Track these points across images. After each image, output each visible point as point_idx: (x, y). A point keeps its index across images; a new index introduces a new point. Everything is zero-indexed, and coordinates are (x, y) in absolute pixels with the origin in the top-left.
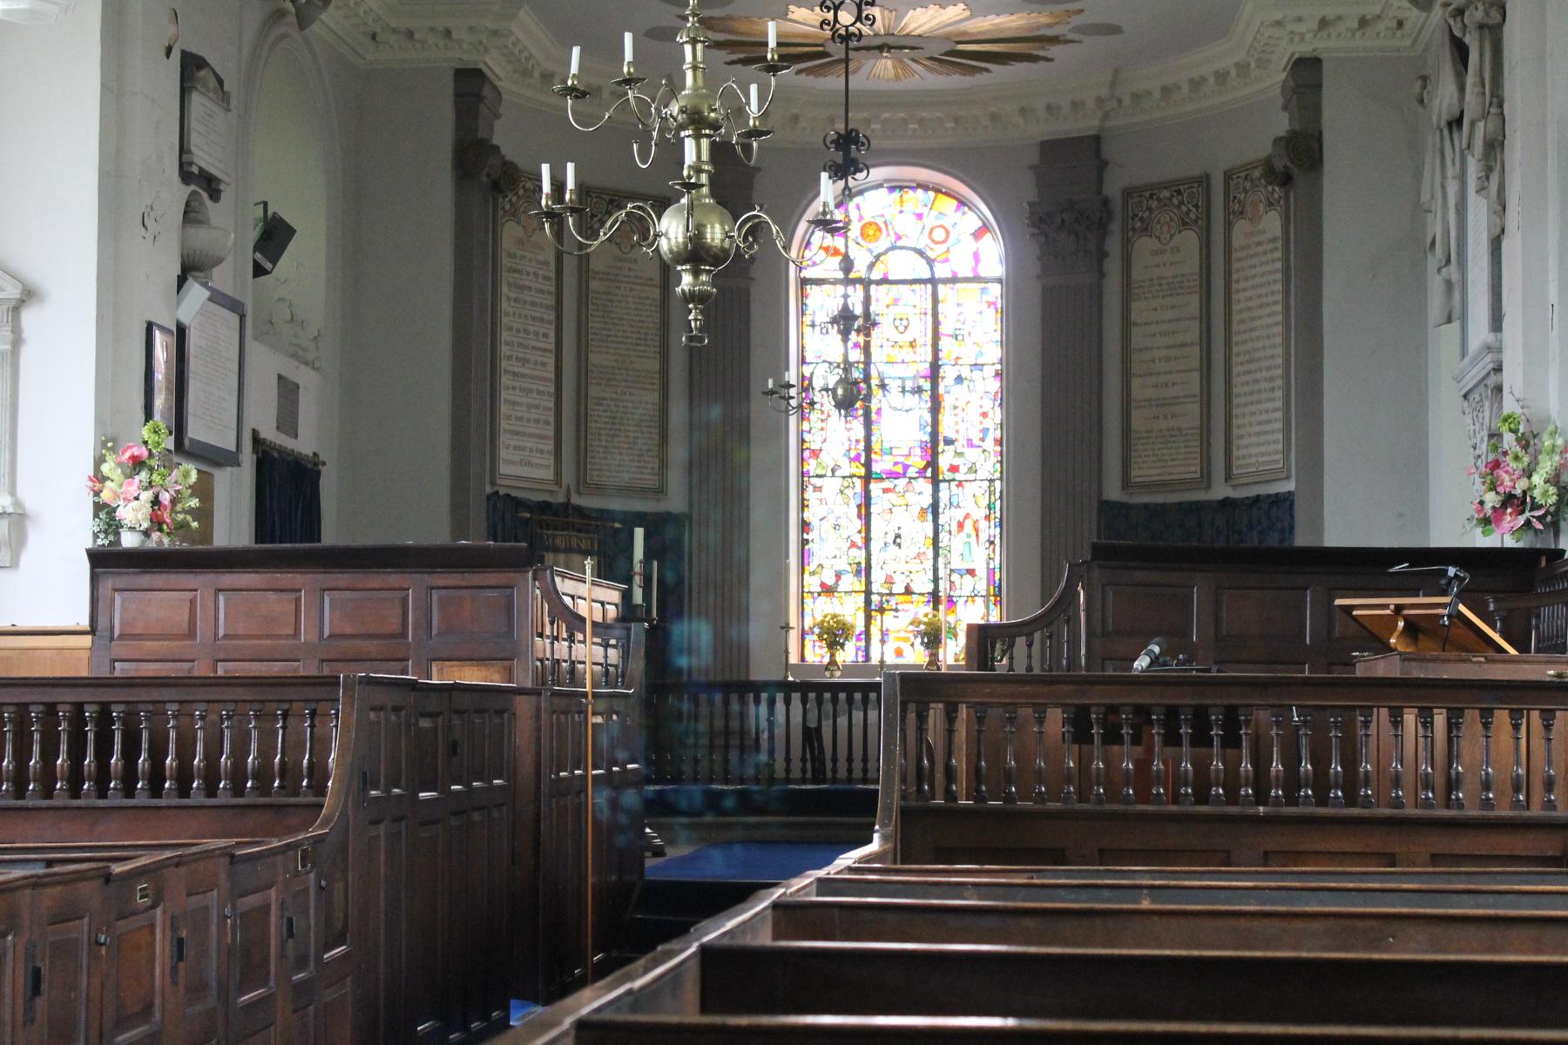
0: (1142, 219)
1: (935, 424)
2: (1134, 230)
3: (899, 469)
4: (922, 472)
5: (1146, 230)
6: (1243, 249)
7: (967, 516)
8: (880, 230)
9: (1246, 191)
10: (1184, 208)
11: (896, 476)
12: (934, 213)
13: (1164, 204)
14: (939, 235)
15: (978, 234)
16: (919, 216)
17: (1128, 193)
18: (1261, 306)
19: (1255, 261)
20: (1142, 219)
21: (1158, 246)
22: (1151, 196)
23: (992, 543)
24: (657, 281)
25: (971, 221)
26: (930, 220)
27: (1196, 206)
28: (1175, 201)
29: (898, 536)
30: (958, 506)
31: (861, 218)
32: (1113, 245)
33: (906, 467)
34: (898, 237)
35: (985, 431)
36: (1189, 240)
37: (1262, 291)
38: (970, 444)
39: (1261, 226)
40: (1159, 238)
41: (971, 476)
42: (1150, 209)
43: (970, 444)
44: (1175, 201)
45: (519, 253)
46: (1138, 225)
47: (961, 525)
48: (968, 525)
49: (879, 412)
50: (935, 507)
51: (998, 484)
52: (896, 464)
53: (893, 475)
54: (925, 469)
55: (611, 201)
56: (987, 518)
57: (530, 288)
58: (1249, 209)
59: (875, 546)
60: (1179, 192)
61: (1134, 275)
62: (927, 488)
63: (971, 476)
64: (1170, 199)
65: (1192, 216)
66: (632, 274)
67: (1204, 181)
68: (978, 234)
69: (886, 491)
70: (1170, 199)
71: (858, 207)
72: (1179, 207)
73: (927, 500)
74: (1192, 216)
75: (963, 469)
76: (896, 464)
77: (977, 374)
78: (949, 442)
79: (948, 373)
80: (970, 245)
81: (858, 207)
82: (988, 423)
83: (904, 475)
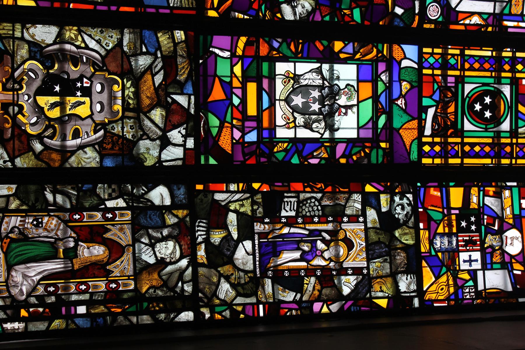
1: (308, 175)
3: (217, 93)
4: (207, 143)
7: (116, 250)
11: (202, 92)
23: (54, 311)
29: (69, 88)
30: (137, 228)
33: (220, 109)
35: (293, 280)
38: (269, 249)
41: (201, 253)
43: (269, 249)
47: (95, 234)
48: (98, 251)
49: (333, 58)
50: (126, 170)
51: (187, 316)
52: (227, 87)
53: (202, 78)
54: (219, 153)
56: (113, 296)
59: (45, 34)
62: (173, 154)
63: (201, 253)
69: (170, 63)
73: (149, 151)
75: (217, 237)
76: (227, 87)
77: (401, 257)
78: (272, 206)
79: (402, 207)
82: (310, 283)
83: (204, 105)
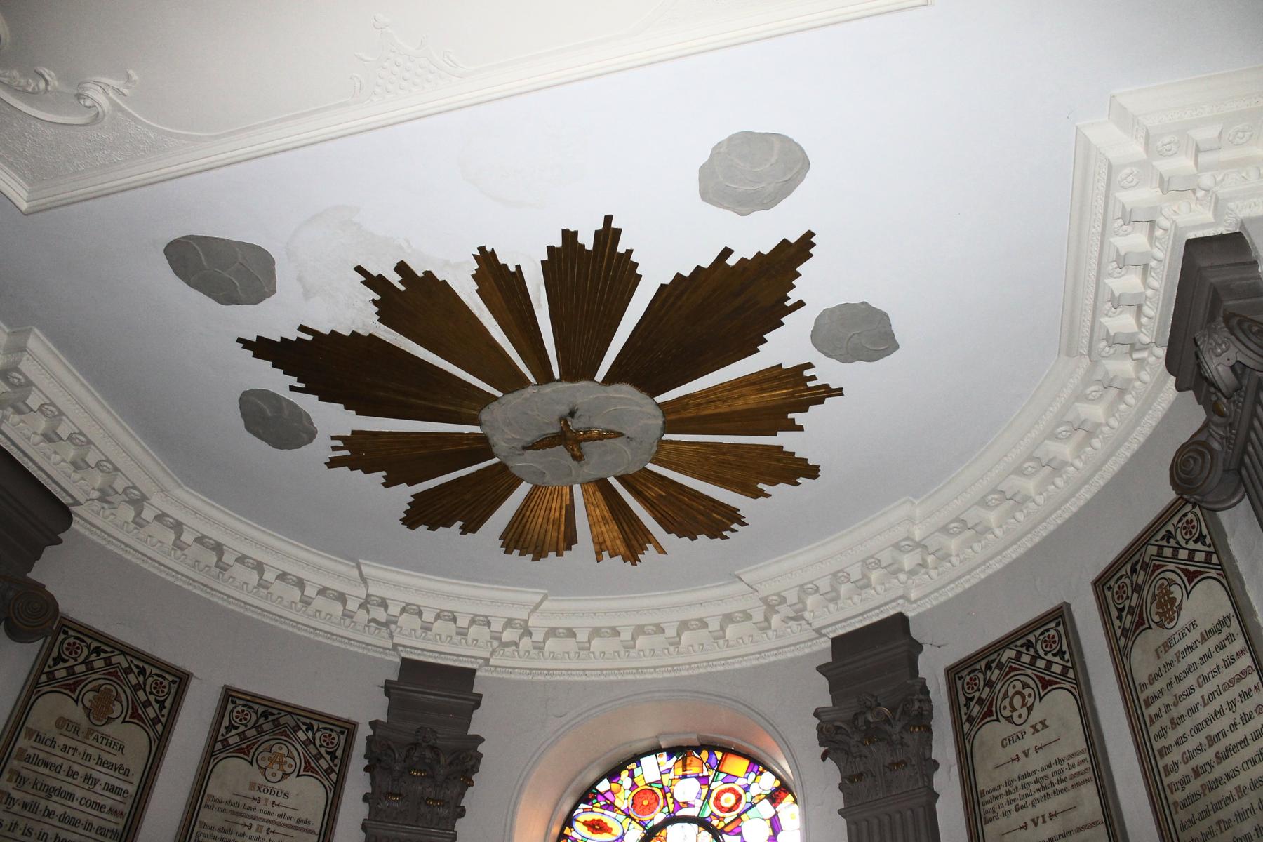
0: (980, 701)
2: (970, 720)
5: (989, 713)
6: (1152, 679)
8: (657, 800)
9: (1137, 589)
10: (1041, 664)
12: (722, 776)
13: (1009, 671)
14: (728, 800)
15: (774, 797)
16: (703, 780)
17: (953, 673)
18: (1229, 751)
19: (1191, 680)
20: (980, 701)
21: (1010, 730)
22: (988, 667)
24: (316, 826)
25: (768, 782)
26: (717, 786)
27: (1061, 654)
28: (1026, 659)
31: (634, 785)
32: (944, 748)
34: (678, 806)
36: (1060, 703)
37: (1223, 723)
39: (1184, 620)
40: (1010, 719)
42: (990, 684)
44: (1026, 659)
45: (62, 740)
46: (976, 710)
55: (265, 715)
57: (70, 796)
58: (1153, 612)
60: (1029, 645)
61: (983, 783)
64: (1018, 658)
65: (1056, 669)
66: (277, 810)
67: (1060, 615)
68: (774, 797)
70: (1018, 658)
71: (632, 775)
72: (1032, 663)
74: (1056, 669)
80: (766, 809)
81: (632, 775)
